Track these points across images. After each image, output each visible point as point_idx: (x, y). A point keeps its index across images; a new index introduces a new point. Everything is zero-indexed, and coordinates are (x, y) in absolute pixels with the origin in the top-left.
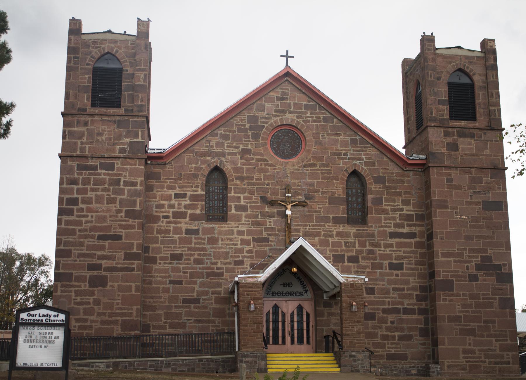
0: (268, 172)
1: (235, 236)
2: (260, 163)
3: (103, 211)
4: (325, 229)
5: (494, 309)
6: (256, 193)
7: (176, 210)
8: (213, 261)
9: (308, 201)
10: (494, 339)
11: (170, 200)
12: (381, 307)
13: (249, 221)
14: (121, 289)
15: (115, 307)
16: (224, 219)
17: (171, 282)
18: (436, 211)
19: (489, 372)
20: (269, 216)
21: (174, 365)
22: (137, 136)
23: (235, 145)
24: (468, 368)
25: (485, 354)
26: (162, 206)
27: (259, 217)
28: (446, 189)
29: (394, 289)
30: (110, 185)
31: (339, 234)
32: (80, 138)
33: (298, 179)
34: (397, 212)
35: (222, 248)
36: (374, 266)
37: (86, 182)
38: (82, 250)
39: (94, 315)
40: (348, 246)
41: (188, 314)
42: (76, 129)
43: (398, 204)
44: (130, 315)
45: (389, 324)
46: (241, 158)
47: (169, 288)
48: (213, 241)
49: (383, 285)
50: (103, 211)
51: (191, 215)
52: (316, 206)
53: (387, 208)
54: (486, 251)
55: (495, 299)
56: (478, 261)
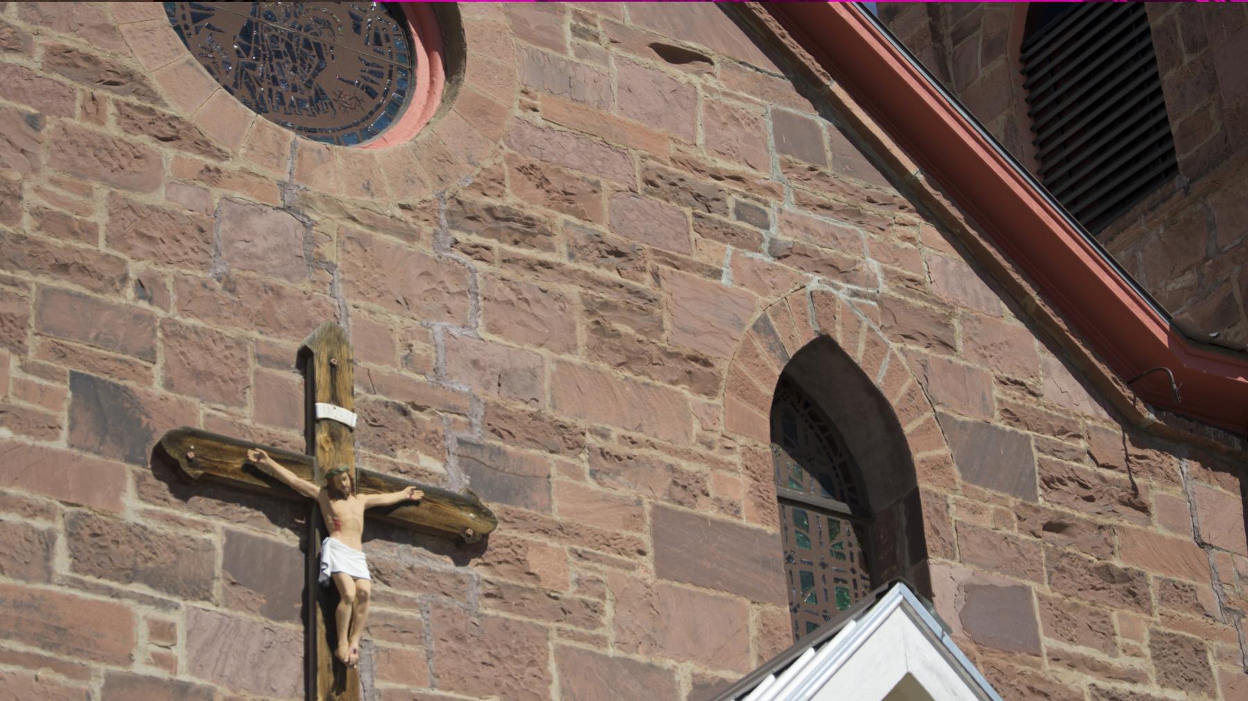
2: (82, 90)
6: (32, 342)
20: (153, 580)
27: (62, 562)
33: (405, 303)
43: (1137, 663)
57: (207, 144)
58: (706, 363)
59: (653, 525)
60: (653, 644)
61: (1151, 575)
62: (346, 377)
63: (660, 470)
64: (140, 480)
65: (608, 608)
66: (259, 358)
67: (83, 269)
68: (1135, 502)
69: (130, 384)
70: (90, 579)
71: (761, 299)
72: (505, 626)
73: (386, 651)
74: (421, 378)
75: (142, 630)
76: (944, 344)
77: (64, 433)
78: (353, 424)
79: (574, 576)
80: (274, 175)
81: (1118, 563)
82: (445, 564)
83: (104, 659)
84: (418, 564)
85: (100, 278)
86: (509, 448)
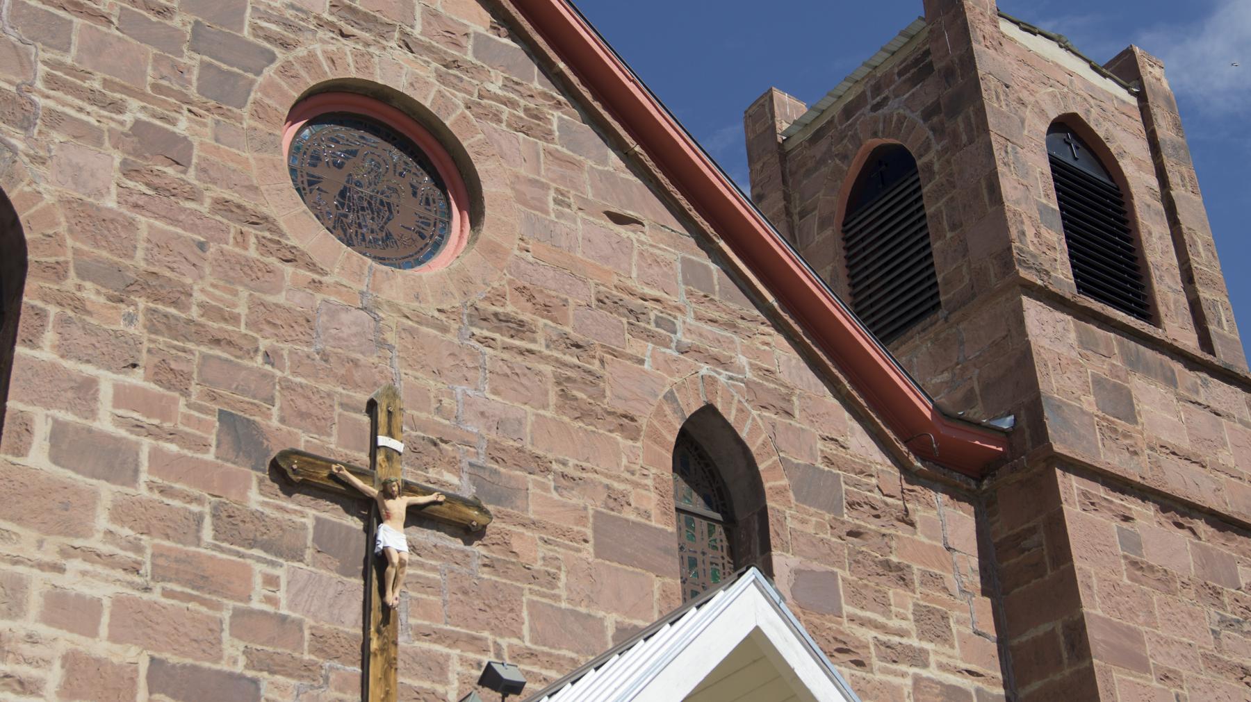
0: (278, 291)
1: (30, 623)
2: (234, 227)
6: (195, 389)
13: (139, 549)
20: (266, 547)
23: (97, 85)
27: (207, 533)
28: (1126, 581)
33: (438, 373)
34: (903, 667)
46: (129, 171)
57: (314, 265)
58: (632, 419)
59: (594, 524)
60: (591, 601)
61: (915, 567)
62: (398, 419)
63: (600, 488)
64: (261, 481)
65: (563, 576)
66: (341, 405)
67: (230, 343)
68: (906, 519)
69: (257, 419)
70: (225, 545)
71: (669, 379)
72: (495, 586)
73: (417, 599)
74: (447, 422)
75: (258, 580)
76: (787, 413)
77: (213, 449)
78: (401, 450)
79: (541, 555)
80: (357, 287)
81: (894, 559)
82: (457, 544)
83: (232, 598)
84: (440, 543)
85: (241, 349)
86: (502, 470)
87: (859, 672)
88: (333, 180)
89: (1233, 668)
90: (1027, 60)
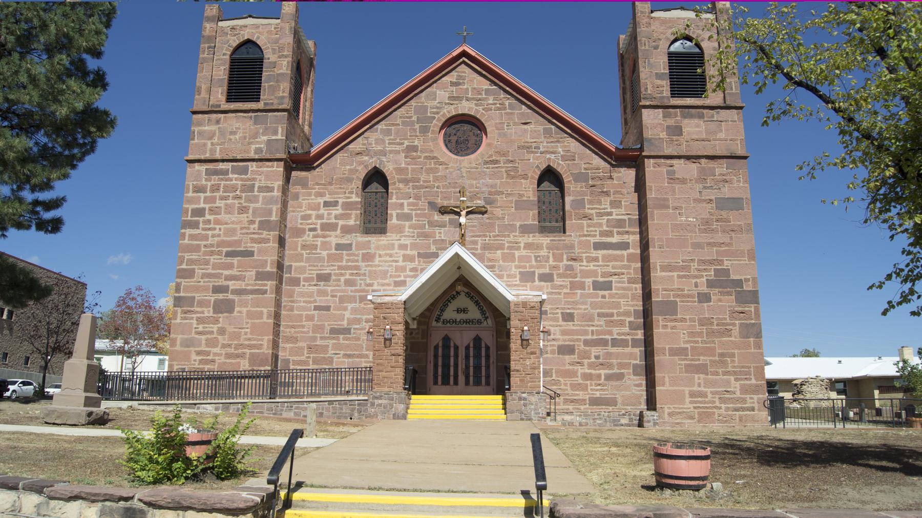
1: (396, 250)
3: (233, 223)
4: (510, 239)
5: (733, 339)
7: (324, 221)
8: (368, 281)
9: (488, 207)
10: (732, 378)
11: (319, 209)
12: (583, 338)
14: (250, 315)
15: (243, 337)
16: (383, 231)
17: (316, 308)
18: (652, 213)
19: (726, 421)
21: (297, 408)
22: (276, 133)
24: (696, 416)
25: (720, 398)
26: (309, 217)
29: (599, 315)
30: (242, 191)
31: (528, 246)
32: (211, 138)
33: (475, 179)
35: (379, 266)
36: (573, 286)
37: (215, 188)
38: (207, 269)
39: (217, 346)
40: (540, 261)
41: (335, 347)
42: (206, 128)
44: (260, 347)
45: (593, 360)
46: (406, 157)
47: (313, 316)
48: (368, 257)
49: (585, 309)
50: (233, 223)
51: (343, 227)
52: (498, 212)
53: (591, 211)
54: (720, 262)
55: (734, 325)
56: (710, 276)
68: (611, 178)
87: (589, 221)
88: (454, 139)
89: (705, 200)
90: (664, 21)
